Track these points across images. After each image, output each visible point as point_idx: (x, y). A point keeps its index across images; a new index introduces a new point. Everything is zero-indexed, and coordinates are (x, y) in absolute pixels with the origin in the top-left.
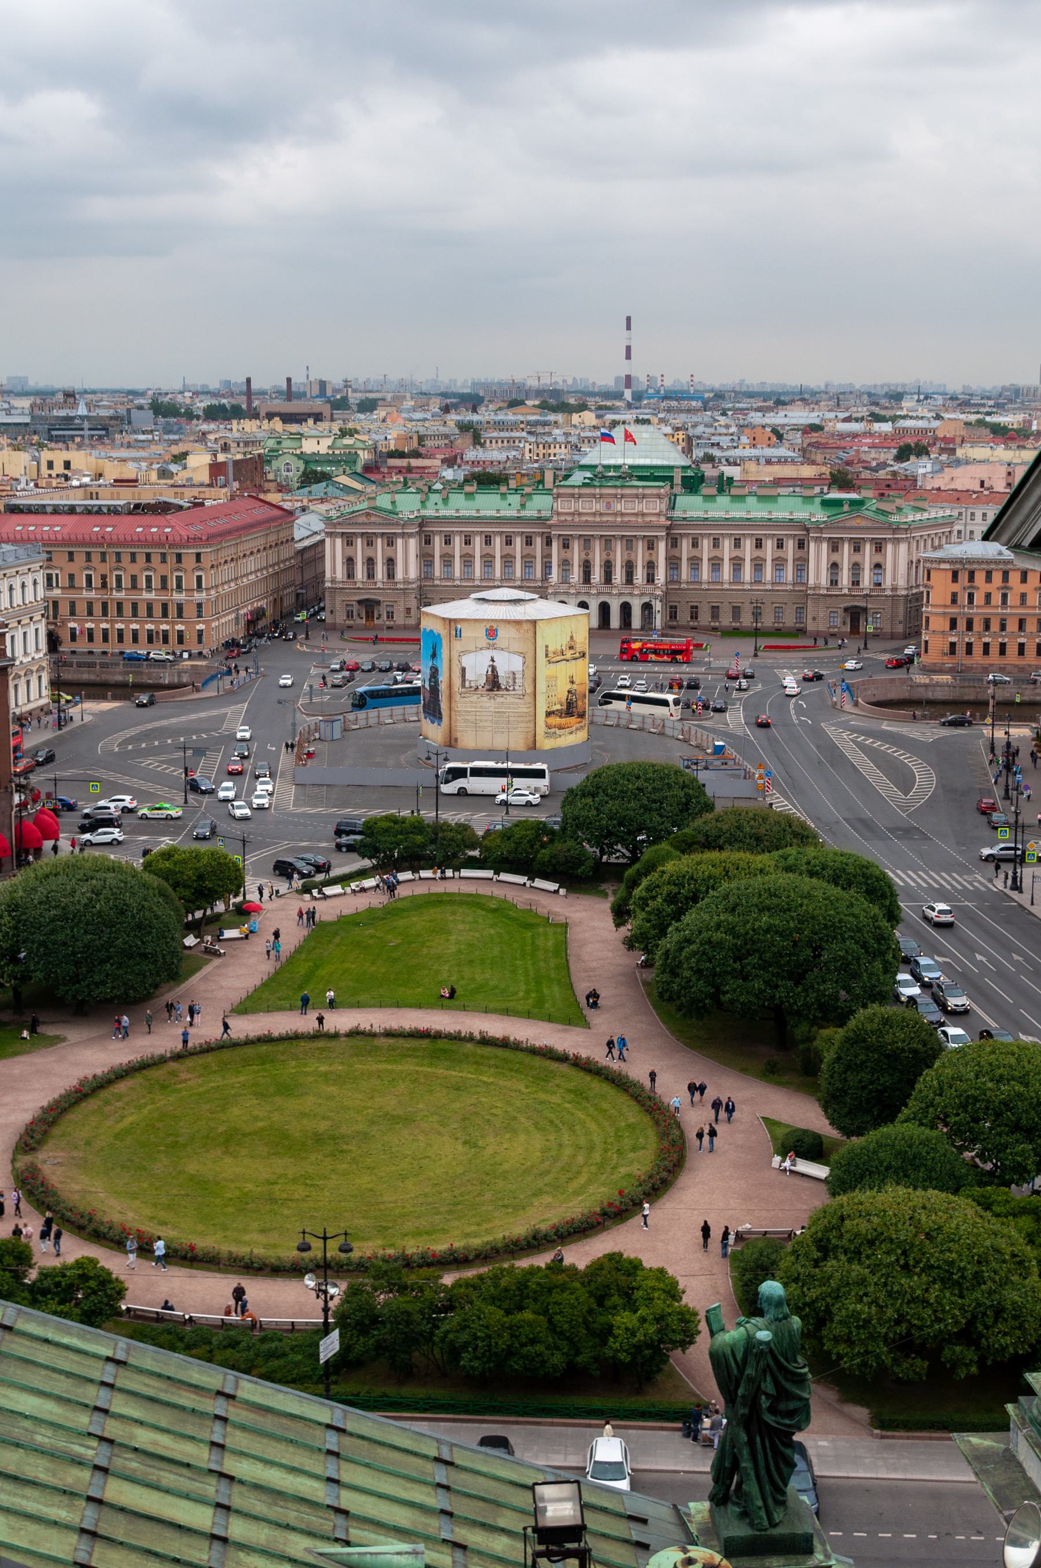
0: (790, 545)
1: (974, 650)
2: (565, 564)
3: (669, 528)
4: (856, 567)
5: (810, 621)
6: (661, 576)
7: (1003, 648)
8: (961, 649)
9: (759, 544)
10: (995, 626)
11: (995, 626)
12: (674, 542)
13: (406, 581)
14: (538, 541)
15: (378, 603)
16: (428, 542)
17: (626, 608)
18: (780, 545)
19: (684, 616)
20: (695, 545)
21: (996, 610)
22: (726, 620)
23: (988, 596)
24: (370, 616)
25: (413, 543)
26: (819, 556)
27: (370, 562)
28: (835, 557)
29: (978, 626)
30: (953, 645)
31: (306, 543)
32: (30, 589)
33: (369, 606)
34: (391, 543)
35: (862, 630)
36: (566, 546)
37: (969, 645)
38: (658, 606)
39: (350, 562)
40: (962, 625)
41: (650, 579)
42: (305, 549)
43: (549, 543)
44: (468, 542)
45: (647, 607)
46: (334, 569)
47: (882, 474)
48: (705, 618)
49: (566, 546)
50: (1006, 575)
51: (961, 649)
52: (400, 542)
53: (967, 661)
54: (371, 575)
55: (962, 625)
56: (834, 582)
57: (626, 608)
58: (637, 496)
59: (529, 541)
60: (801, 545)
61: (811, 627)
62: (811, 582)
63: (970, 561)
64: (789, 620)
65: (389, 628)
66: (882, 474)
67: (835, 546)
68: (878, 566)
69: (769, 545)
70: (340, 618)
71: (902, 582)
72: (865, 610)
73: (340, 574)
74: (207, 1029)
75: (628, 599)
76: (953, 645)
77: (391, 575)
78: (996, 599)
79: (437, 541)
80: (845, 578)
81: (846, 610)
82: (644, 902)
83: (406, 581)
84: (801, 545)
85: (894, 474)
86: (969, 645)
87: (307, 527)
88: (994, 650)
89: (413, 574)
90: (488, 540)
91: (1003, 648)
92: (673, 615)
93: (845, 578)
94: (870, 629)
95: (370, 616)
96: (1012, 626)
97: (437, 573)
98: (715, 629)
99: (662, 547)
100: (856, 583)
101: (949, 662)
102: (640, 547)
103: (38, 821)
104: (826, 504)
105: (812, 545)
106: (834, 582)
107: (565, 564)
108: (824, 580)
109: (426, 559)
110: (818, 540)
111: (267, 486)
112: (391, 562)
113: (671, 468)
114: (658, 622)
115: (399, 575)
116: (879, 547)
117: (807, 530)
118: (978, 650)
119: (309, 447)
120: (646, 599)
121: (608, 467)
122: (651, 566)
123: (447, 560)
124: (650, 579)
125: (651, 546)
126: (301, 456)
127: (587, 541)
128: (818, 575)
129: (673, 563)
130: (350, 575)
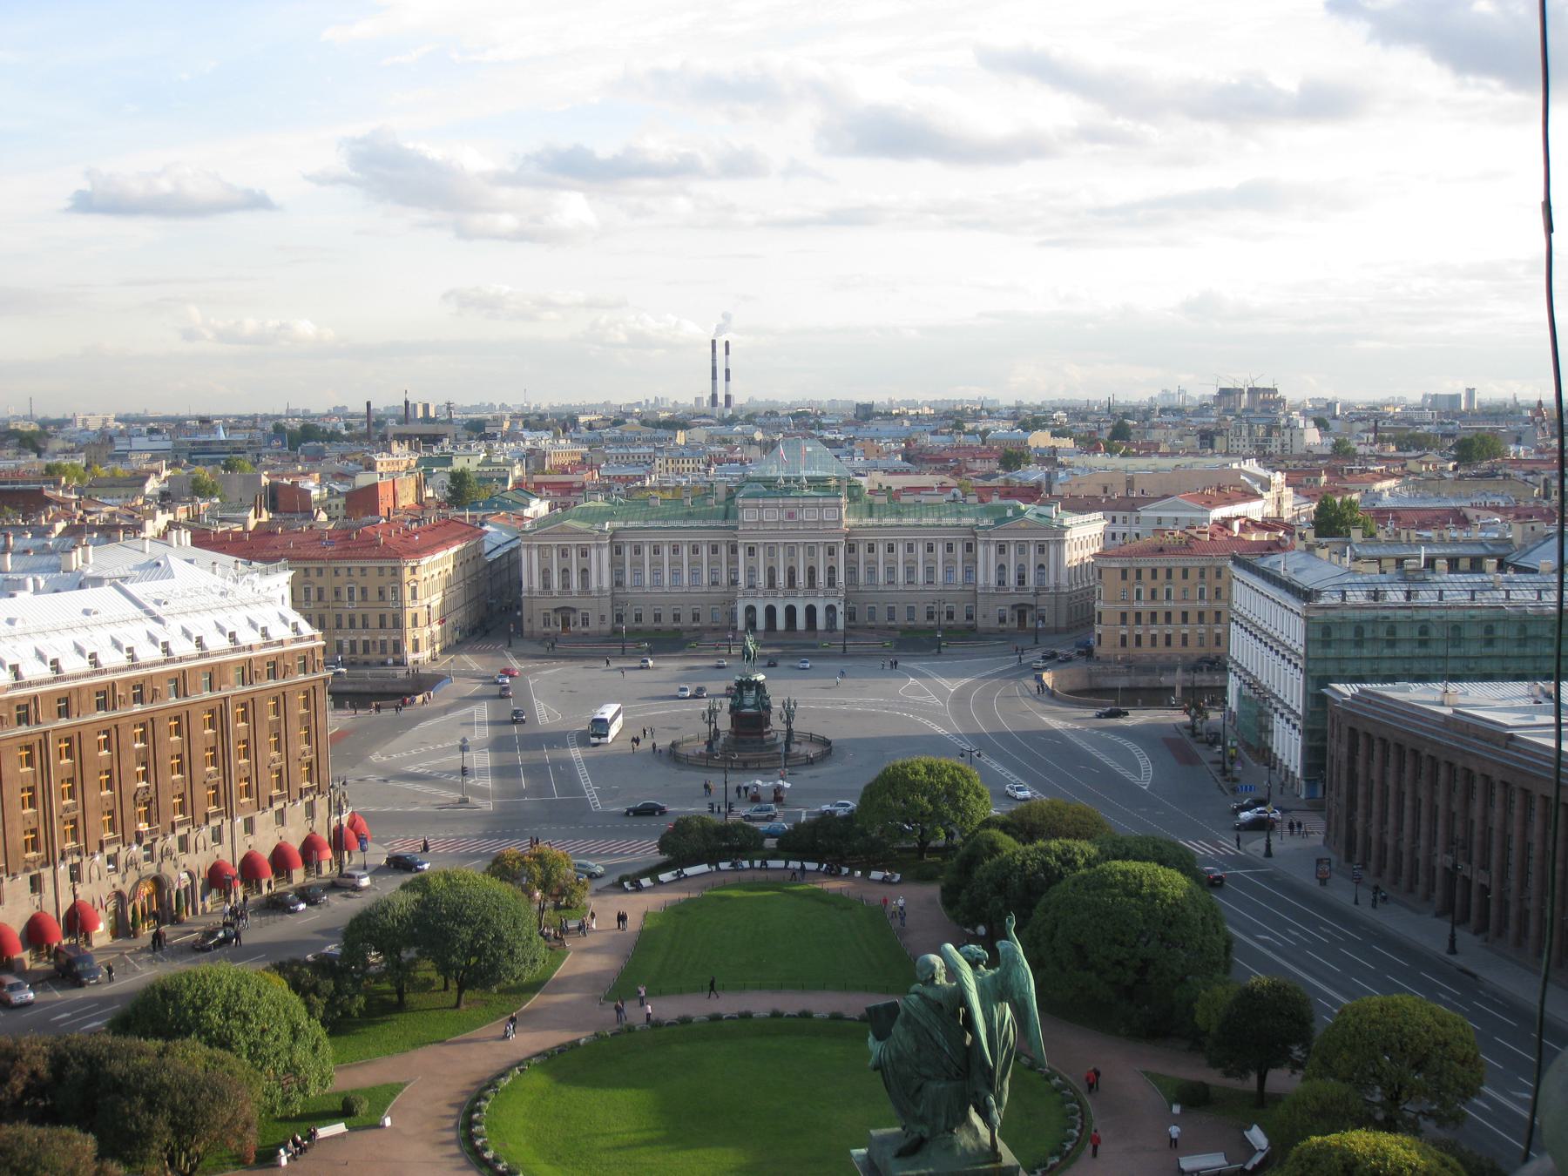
0: (959, 549)
1: (1173, 641)
2: (751, 572)
6: (841, 577)
7: (1168, 637)
8: (1131, 642)
10: (1161, 618)
11: (1161, 618)
12: (851, 548)
13: (600, 590)
14: (724, 548)
15: (574, 610)
16: (618, 551)
17: (811, 611)
18: (950, 548)
19: (862, 618)
20: (871, 549)
21: (1162, 605)
23: (1153, 593)
24: (566, 623)
25: (606, 553)
26: (986, 557)
27: (565, 572)
29: (1145, 618)
30: (1124, 638)
31: (496, 555)
33: (565, 613)
34: (584, 554)
35: (1029, 624)
36: (751, 551)
37: (1138, 638)
38: (840, 609)
39: (546, 574)
40: (1131, 618)
41: (831, 582)
42: (495, 560)
43: (734, 550)
44: (656, 551)
46: (531, 578)
47: (993, 482)
49: (751, 551)
50: (1169, 572)
51: (1131, 642)
52: (594, 552)
53: (1138, 651)
55: (1131, 618)
56: (1001, 583)
57: (811, 611)
58: (817, 505)
59: (715, 550)
60: (969, 547)
61: (981, 623)
62: (981, 581)
64: (960, 619)
65: (586, 634)
66: (993, 482)
67: (1002, 549)
68: (1041, 566)
69: (940, 549)
71: (1064, 581)
72: (1031, 607)
73: (536, 585)
75: (771, 602)
76: (1124, 638)
78: (1162, 594)
79: (628, 551)
81: (1013, 607)
83: (600, 590)
84: (969, 547)
86: (1138, 638)
88: (1161, 641)
89: (606, 584)
90: (676, 550)
91: (1168, 637)
92: (851, 615)
95: (566, 623)
96: (1176, 618)
97: (628, 581)
98: (891, 628)
101: (1120, 653)
102: (821, 553)
103: (352, 824)
104: (990, 511)
105: (980, 549)
107: (751, 572)
108: (993, 581)
110: (987, 543)
112: (585, 572)
114: (841, 623)
115: (594, 585)
116: (1042, 549)
117: (975, 534)
118: (1146, 641)
119: (459, 464)
120: (834, 602)
121: (787, 480)
122: (832, 570)
123: (638, 566)
124: (831, 582)
125: (831, 552)
127: (771, 550)
128: (986, 575)
129: (852, 571)
130: (547, 585)
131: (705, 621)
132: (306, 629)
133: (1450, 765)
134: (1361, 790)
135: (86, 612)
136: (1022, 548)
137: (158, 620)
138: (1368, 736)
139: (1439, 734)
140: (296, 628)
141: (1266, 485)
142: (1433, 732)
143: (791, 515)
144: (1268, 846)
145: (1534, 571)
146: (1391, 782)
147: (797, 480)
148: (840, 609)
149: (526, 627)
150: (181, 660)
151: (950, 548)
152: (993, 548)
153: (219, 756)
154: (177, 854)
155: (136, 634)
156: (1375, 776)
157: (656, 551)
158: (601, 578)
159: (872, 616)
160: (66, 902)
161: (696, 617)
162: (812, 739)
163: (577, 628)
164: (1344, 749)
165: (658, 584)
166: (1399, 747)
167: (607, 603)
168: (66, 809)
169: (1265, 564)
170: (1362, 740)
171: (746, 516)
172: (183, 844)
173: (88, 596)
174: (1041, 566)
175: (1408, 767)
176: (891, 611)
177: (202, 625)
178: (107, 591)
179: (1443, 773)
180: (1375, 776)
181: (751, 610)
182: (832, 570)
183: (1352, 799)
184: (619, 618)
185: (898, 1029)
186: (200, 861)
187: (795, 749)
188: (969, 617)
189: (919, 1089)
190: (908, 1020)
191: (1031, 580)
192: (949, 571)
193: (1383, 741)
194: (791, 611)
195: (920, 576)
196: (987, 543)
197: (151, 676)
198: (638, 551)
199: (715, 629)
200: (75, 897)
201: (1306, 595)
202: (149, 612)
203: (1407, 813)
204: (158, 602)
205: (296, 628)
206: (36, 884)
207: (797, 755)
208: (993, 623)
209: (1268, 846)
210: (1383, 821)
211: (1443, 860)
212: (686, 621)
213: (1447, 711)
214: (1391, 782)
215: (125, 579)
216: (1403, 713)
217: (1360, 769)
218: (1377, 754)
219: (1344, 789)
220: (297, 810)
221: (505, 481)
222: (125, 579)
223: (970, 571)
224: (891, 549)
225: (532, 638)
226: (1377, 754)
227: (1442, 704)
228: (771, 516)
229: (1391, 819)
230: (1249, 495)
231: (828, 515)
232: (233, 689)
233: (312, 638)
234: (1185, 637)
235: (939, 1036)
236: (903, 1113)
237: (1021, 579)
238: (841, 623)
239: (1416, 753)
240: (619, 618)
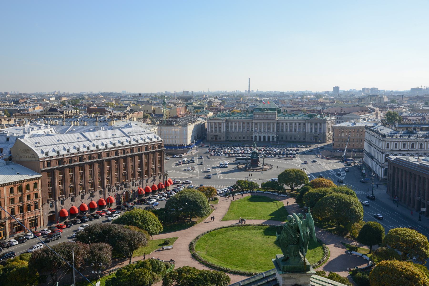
0: (302, 124)
3: (277, 121)
4: (316, 129)
5: (306, 139)
9: (295, 124)
13: (223, 132)
16: (227, 124)
18: (300, 124)
19: (280, 139)
22: (289, 139)
24: (216, 139)
25: (225, 124)
26: (308, 126)
27: (216, 128)
28: (312, 126)
33: (216, 137)
34: (220, 124)
35: (317, 141)
36: (256, 124)
39: (212, 128)
41: (273, 131)
43: (252, 123)
44: (236, 124)
45: (273, 137)
48: (284, 139)
49: (256, 124)
54: (216, 130)
56: (311, 131)
59: (248, 123)
60: (304, 124)
61: (307, 140)
62: (307, 131)
63: (343, 127)
64: (302, 139)
67: (311, 124)
68: (320, 128)
69: (298, 124)
70: (210, 139)
73: (210, 130)
74: (217, 223)
75: (260, 135)
77: (220, 131)
80: (314, 131)
82: (306, 197)
83: (223, 132)
84: (304, 124)
85: (313, 109)
87: (201, 121)
89: (225, 130)
92: (278, 138)
93: (314, 131)
94: (320, 141)
95: (216, 139)
96: (352, 140)
98: (286, 141)
99: (276, 124)
100: (316, 132)
105: (307, 124)
106: (311, 131)
108: (309, 131)
109: (227, 126)
110: (308, 123)
112: (220, 128)
114: (275, 140)
115: (222, 130)
116: (321, 124)
121: (264, 109)
122: (273, 129)
124: (273, 131)
125: (273, 124)
126: (193, 106)
128: (308, 130)
129: (278, 129)
131: (246, 139)
132: (160, 139)
133: (419, 176)
134: (396, 181)
135: (113, 135)
136: (316, 124)
137: (128, 136)
138: (398, 168)
139: (416, 169)
140: (158, 139)
141: (374, 110)
142: (414, 168)
143: (265, 116)
144: (373, 193)
146: (404, 180)
147: (266, 109)
148: (275, 136)
149: (207, 139)
150: (133, 145)
151: (300, 124)
152: (309, 124)
153: (141, 166)
154: (131, 187)
155: (123, 140)
156: (400, 178)
157: (236, 124)
158: (223, 129)
159: (282, 138)
160: (107, 196)
161: (244, 138)
162: (268, 165)
163: (219, 140)
164: (392, 171)
165: (236, 130)
166: (406, 171)
167: (225, 134)
168: (108, 176)
169: (372, 129)
170: (396, 169)
171: (256, 116)
172: (133, 185)
173: (114, 132)
174: (320, 128)
175: (408, 176)
176: (286, 138)
177: (138, 138)
178: (118, 130)
179: (417, 178)
180: (400, 178)
181: (256, 136)
182: (273, 129)
183: (394, 183)
184: (227, 138)
185: (283, 232)
186: (136, 189)
187: (264, 167)
188: (304, 139)
189: (287, 246)
190: (285, 230)
191: (318, 131)
192: (299, 129)
193: (402, 170)
194: (264, 137)
195: (293, 130)
196: (308, 123)
197: (127, 149)
198: (232, 123)
199: (248, 141)
200: (109, 195)
201: (384, 136)
203: (408, 187)
204: (128, 133)
205: (158, 139)
206: (101, 192)
207: (265, 168)
208: (309, 141)
209: (373, 193)
210: (402, 188)
211: (417, 198)
212: (242, 139)
213: (418, 163)
214: (404, 180)
215: (122, 128)
216: (407, 163)
217: (396, 176)
218: (400, 173)
219: (391, 180)
220: (157, 178)
221: (203, 108)
222: (122, 128)
223: (304, 128)
224: (287, 124)
225: (208, 142)
226: (400, 173)
227: (417, 162)
228: (261, 116)
229: (403, 188)
231: (273, 116)
232: (144, 151)
233: (161, 141)
234: (353, 144)
235: (292, 234)
236: (283, 251)
237: (316, 132)
238: (275, 140)
239: (410, 173)
240: (227, 138)
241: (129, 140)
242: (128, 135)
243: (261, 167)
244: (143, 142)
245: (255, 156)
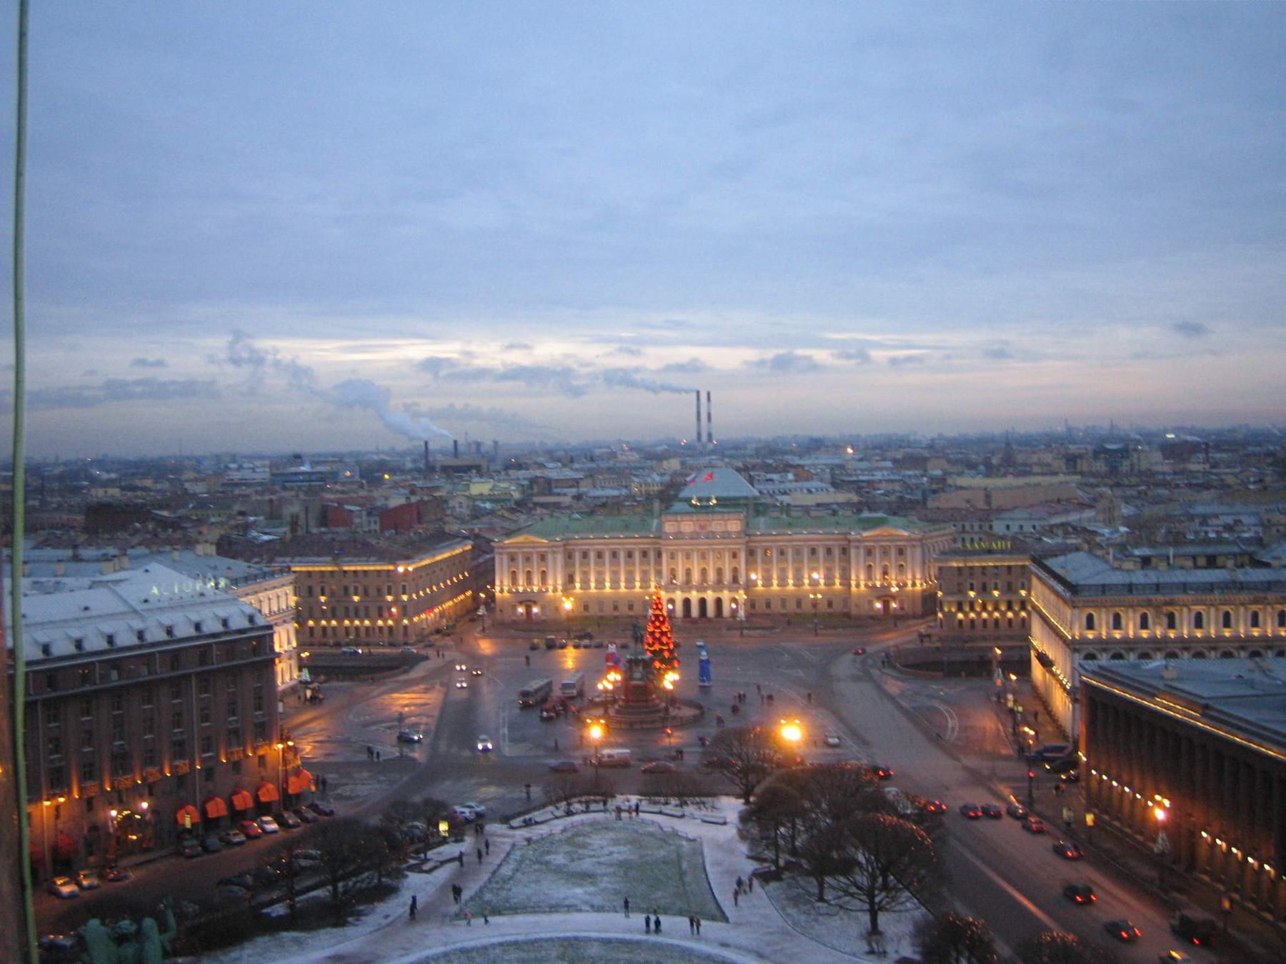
32: (283, 600)
36: (672, 556)
43: (659, 555)
49: (672, 556)
110: (858, 547)
111: (446, 519)
113: (746, 498)
125: (734, 556)
126: (469, 497)
145: (1267, 565)
150: (153, 645)
182: (735, 570)
201: (1073, 588)
202: (131, 606)
207: (674, 718)
222: (117, 582)
230: (1082, 506)
241: (137, 624)
242: (138, 608)
243: (661, 715)
244: (191, 632)
245: (637, 675)
